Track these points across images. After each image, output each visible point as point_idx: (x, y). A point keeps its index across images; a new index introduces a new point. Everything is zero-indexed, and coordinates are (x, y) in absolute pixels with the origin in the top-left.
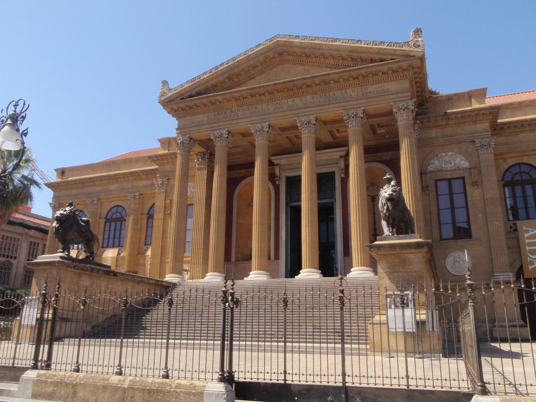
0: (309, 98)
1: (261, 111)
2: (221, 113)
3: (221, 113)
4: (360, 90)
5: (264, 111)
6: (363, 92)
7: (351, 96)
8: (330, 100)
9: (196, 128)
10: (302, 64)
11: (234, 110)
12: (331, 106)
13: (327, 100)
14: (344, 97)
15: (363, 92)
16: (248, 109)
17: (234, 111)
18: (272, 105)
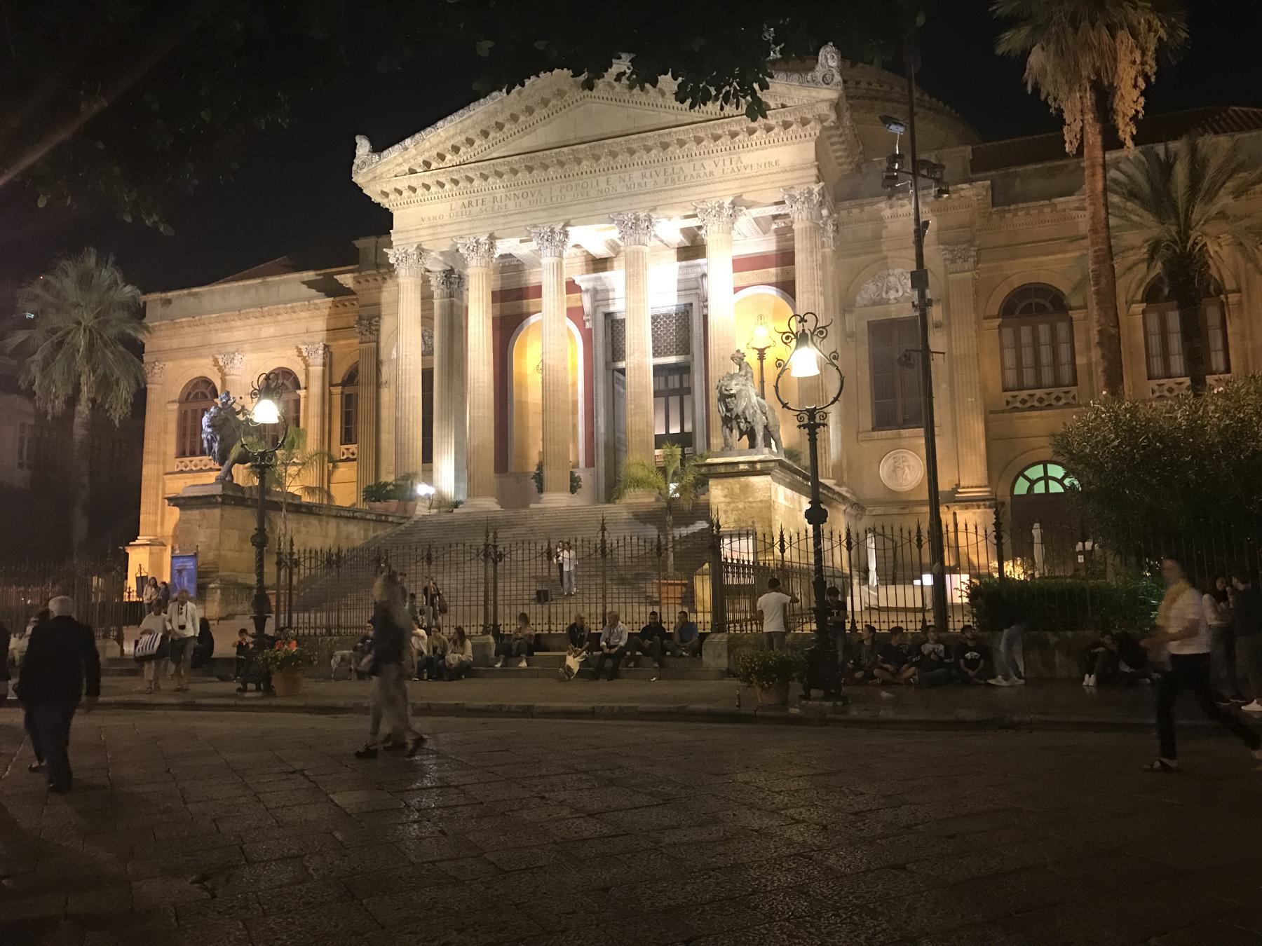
1: (548, 200)
2: (474, 203)
3: (474, 203)
4: (728, 162)
9: (431, 231)
11: (498, 196)
14: (698, 176)
15: (734, 165)
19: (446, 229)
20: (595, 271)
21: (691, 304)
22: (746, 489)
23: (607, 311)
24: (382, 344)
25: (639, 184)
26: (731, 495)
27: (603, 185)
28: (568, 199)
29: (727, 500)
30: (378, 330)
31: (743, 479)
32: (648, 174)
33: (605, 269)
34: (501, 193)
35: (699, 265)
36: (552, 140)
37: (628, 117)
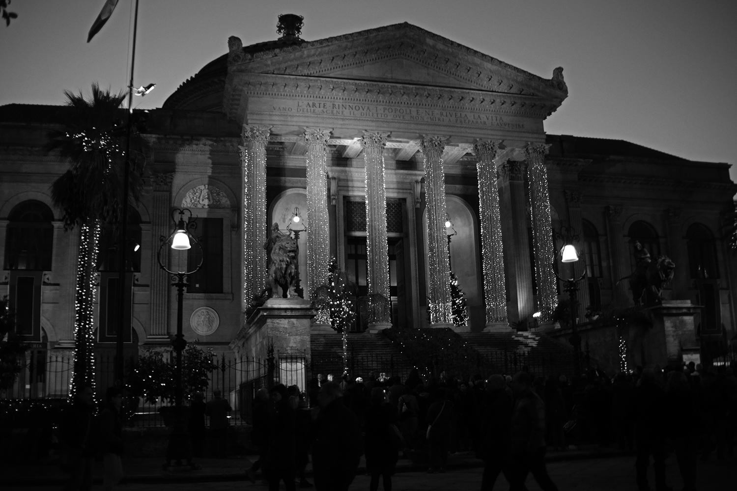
0: (437, 112)
1: (375, 115)
2: (317, 105)
3: (317, 105)
4: (494, 119)
5: (379, 116)
6: (498, 122)
7: (485, 123)
8: (461, 122)
9: (282, 118)
10: (426, 67)
12: (463, 130)
13: (459, 121)
14: (477, 122)
16: (357, 108)
17: (337, 106)
18: (390, 111)
19: (295, 119)
20: (338, 165)
21: (404, 200)
22: (683, 323)
23: (346, 194)
24: (174, 194)
25: (439, 119)
26: (675, 326)
27: (414, 114)
28: (389, 117)
29: (674, 329)
30: (171, 182)
31: (680, 318)
32: (445, 114)
33: (346, 165)
34: (338, 102)
35: (416, 175)
36: (375, 75)
37: (428, 74)
